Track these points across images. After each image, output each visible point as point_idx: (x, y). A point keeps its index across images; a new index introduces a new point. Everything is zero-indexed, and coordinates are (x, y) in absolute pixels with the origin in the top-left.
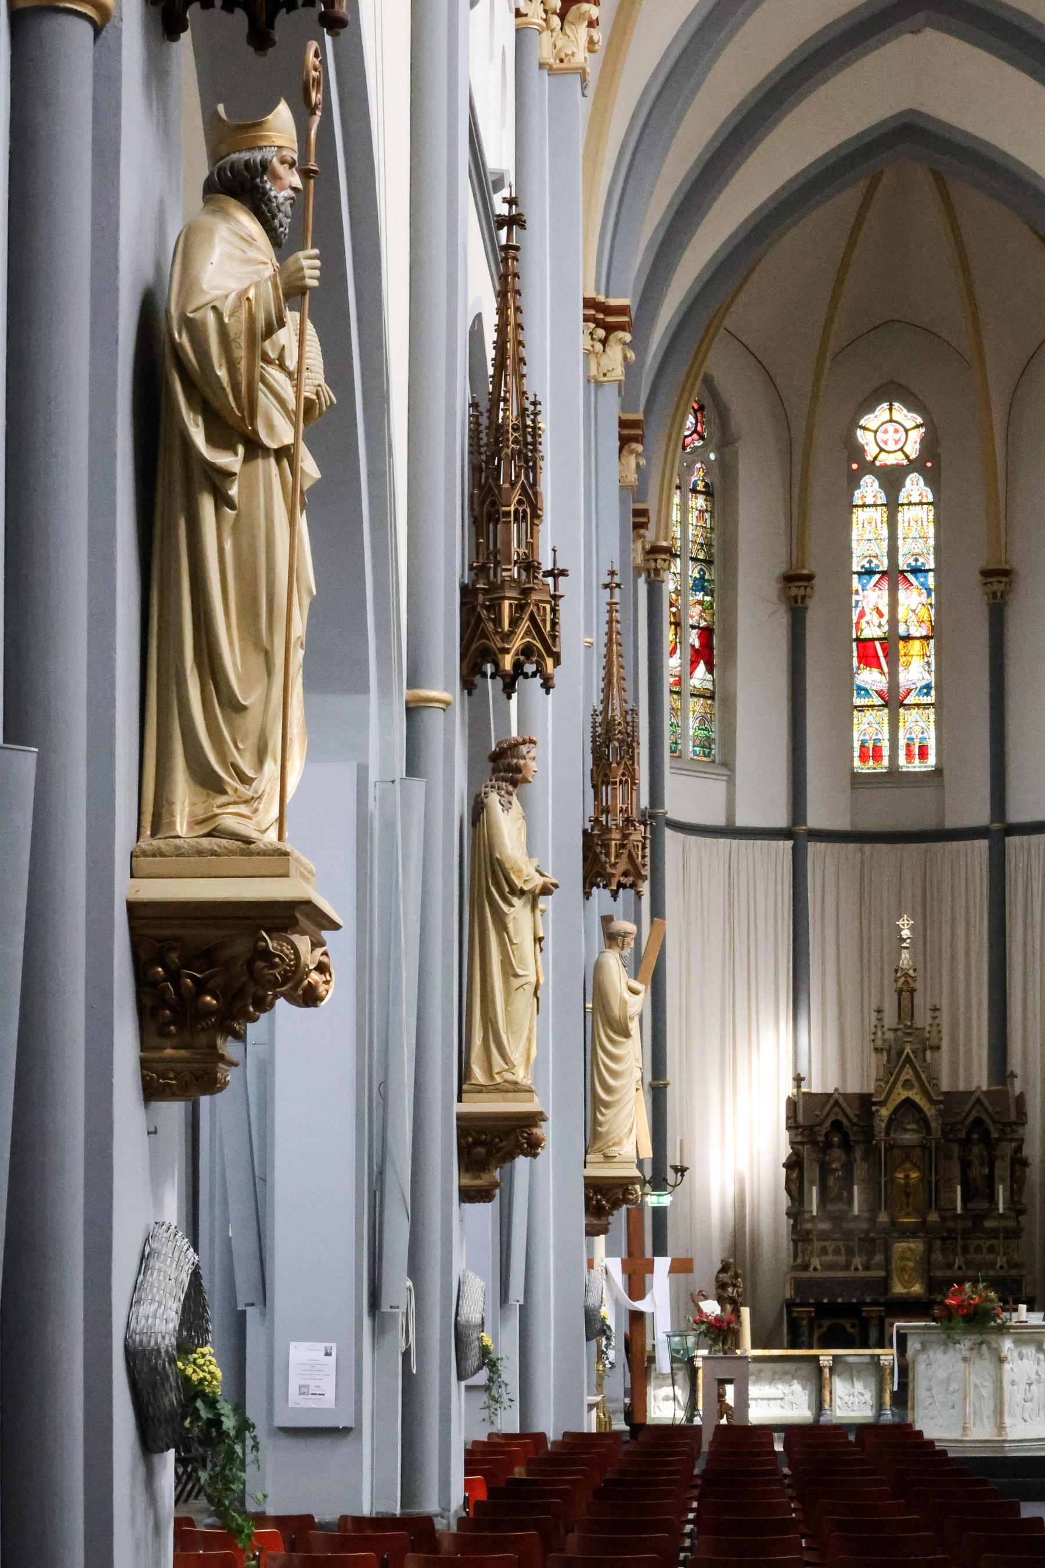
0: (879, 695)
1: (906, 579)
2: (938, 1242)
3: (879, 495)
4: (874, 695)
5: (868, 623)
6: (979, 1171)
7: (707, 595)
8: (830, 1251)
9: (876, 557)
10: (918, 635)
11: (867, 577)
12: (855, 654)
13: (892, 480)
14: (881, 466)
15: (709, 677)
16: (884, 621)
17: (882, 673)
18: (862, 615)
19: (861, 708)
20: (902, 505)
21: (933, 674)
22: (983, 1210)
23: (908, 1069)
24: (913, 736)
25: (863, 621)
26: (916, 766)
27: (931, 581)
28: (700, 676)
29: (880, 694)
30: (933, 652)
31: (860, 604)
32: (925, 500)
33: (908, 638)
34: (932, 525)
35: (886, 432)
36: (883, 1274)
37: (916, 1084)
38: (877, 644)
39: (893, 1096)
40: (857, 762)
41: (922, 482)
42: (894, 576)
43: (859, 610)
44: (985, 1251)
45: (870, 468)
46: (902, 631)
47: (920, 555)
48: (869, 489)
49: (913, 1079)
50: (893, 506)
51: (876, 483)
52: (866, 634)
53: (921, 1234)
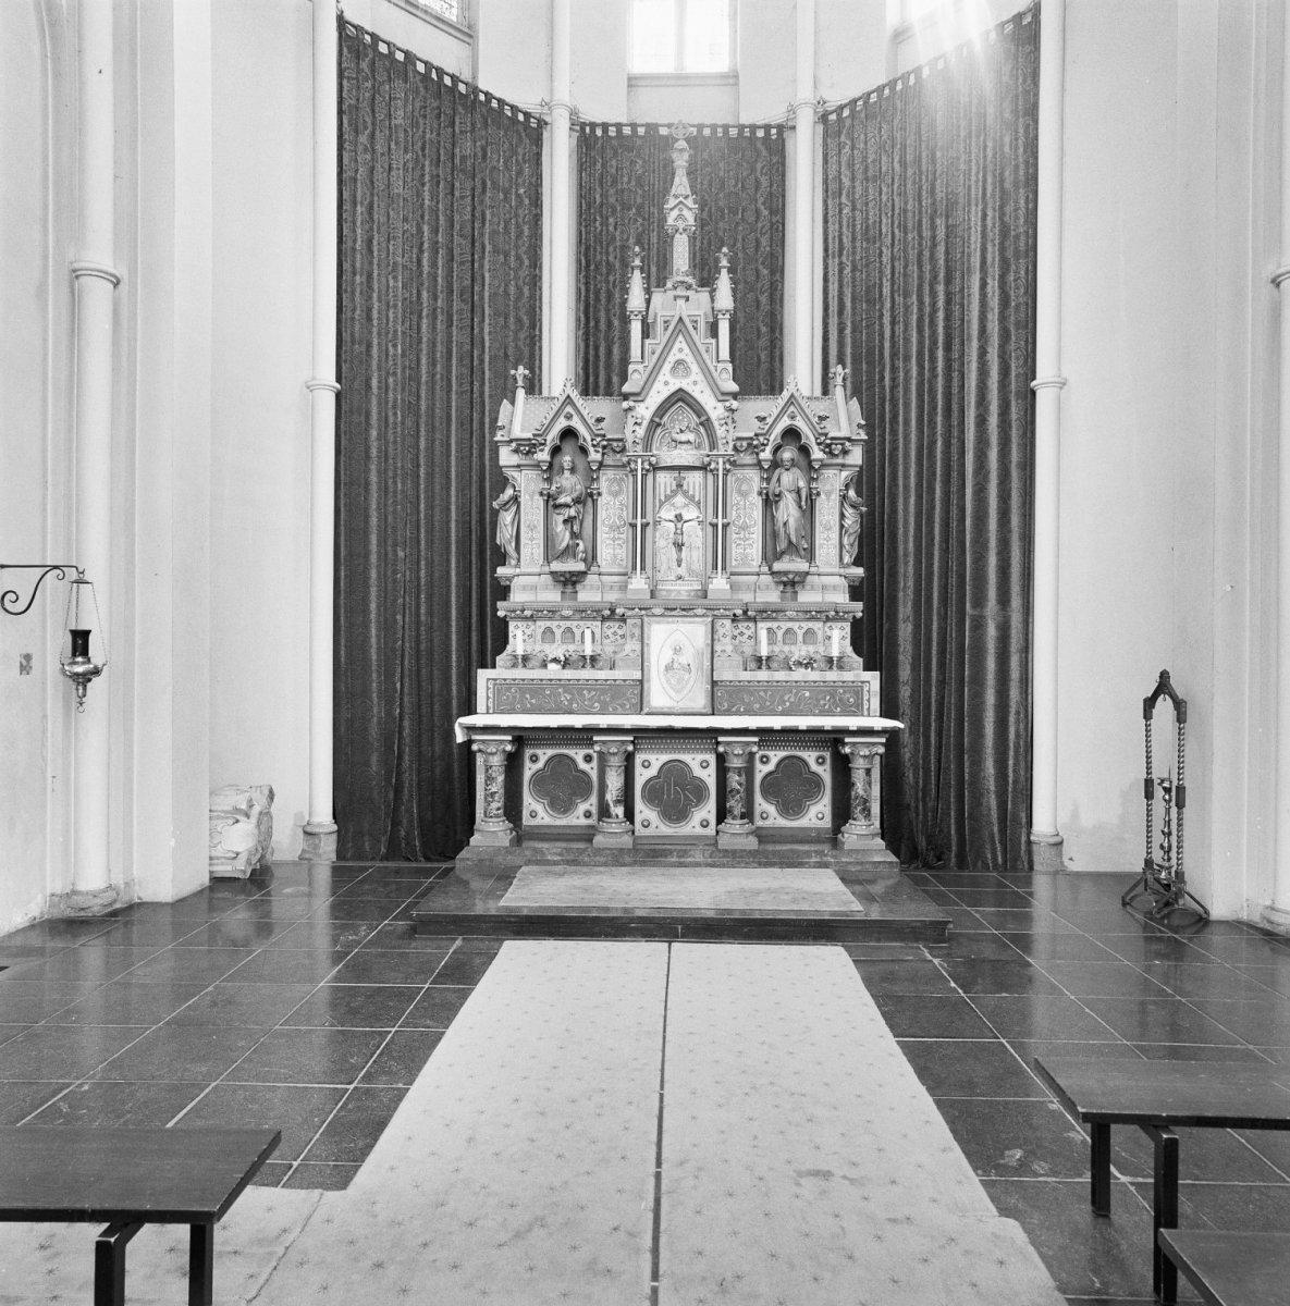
2: (728, 623)
6: (788, 511)
8: (558, 633)
22: (796, 573)
23: (680, 343)
36: (638, 675)
37: (695, 368)
39: (658, 385)
44: (800, 638)
49: (690, 359)
53: (700, 611)
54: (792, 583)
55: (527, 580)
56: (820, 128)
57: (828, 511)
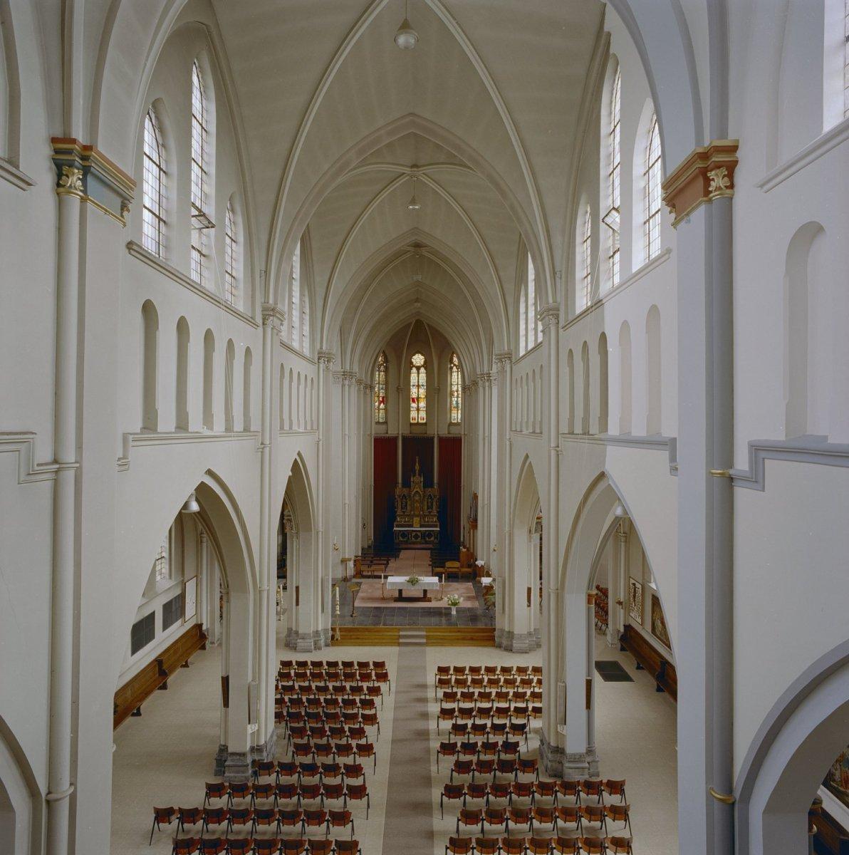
26: (422, 422)
28: (382, 406)
45: (414, 366)
48: (414, 370)
50: (418, 373)
52: (413, 397)
54: (430, 512)
55: (399, 512)
57: (434, 504)
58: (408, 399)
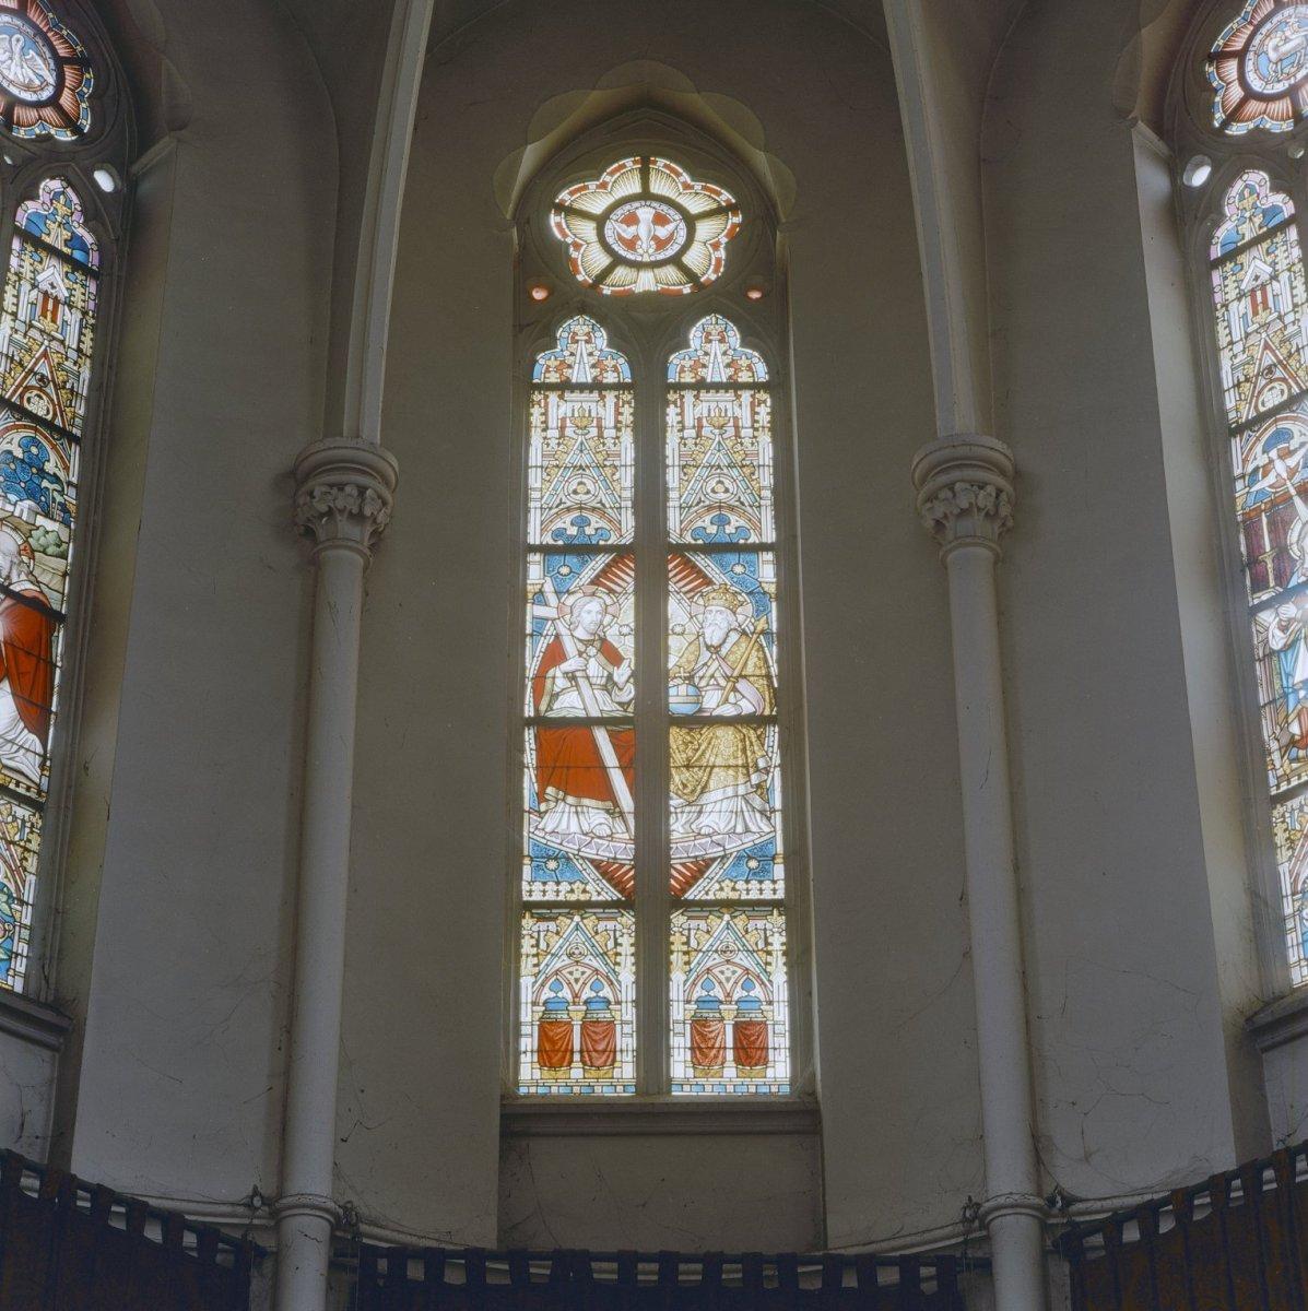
0: (604, 874)
1: (688, 564)
3: (610, 363)
4: (591, 874)
5: (571, 677)
7: (47, 515)
9: (600, 510)
10: (728, 711)
11: (572, 560)
12: (530, 757)
13: (647, 330)
14: (615, 297)
15: (32, 740)
16: (622, 674)
17: (615, 811)
18: (555, 655)
19: (547, 910)
20: (680, 387)
21: (778, 819)
24: (718, 993)
25: (557, 672)
26: (729, 1080)
27: (767, 571)
29: (605, 870)
30: (777, 760)
31: (549, 628)
32: (744, 377)
33: (697, 721)
34: (765, 439)
35: (632, 220)
38: (601, 737)
40: (530, 1075)
41: (734, 337)
42: (652, 559)
43: (543, 644)
46: (678, 699)
47: (732, 508)
48: (582, 348)
50: (650, 394)
51: (601, 338)
52: (570, 704)
56: (1062, 1270)
58: (470, 739)
